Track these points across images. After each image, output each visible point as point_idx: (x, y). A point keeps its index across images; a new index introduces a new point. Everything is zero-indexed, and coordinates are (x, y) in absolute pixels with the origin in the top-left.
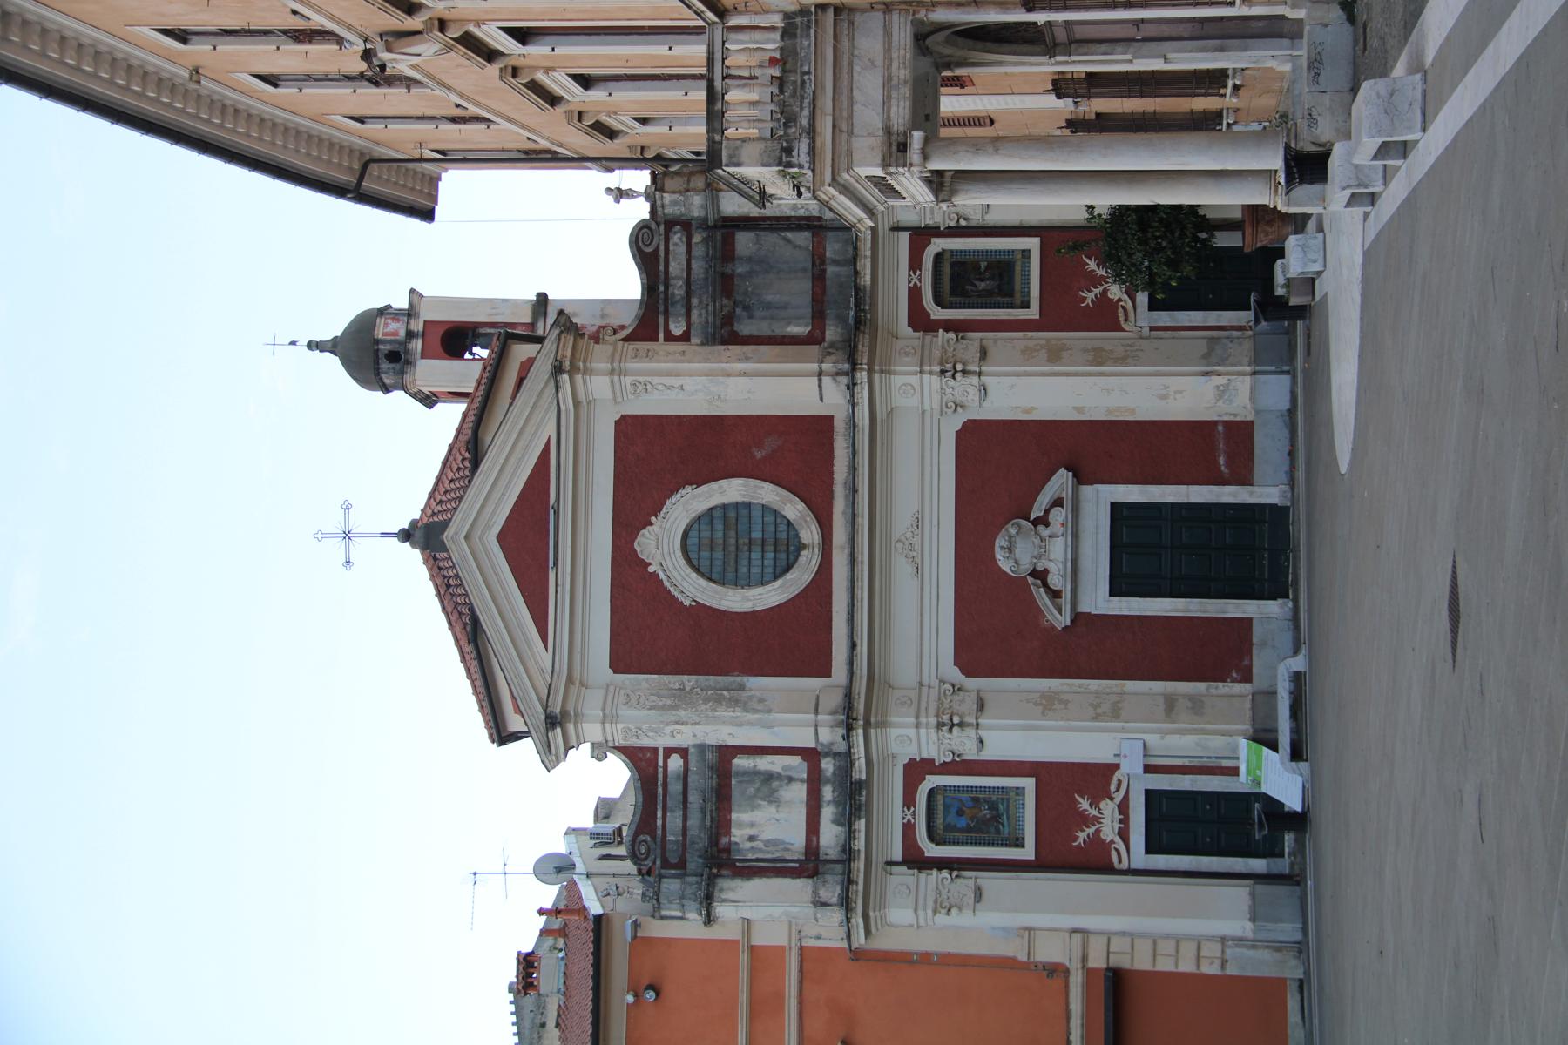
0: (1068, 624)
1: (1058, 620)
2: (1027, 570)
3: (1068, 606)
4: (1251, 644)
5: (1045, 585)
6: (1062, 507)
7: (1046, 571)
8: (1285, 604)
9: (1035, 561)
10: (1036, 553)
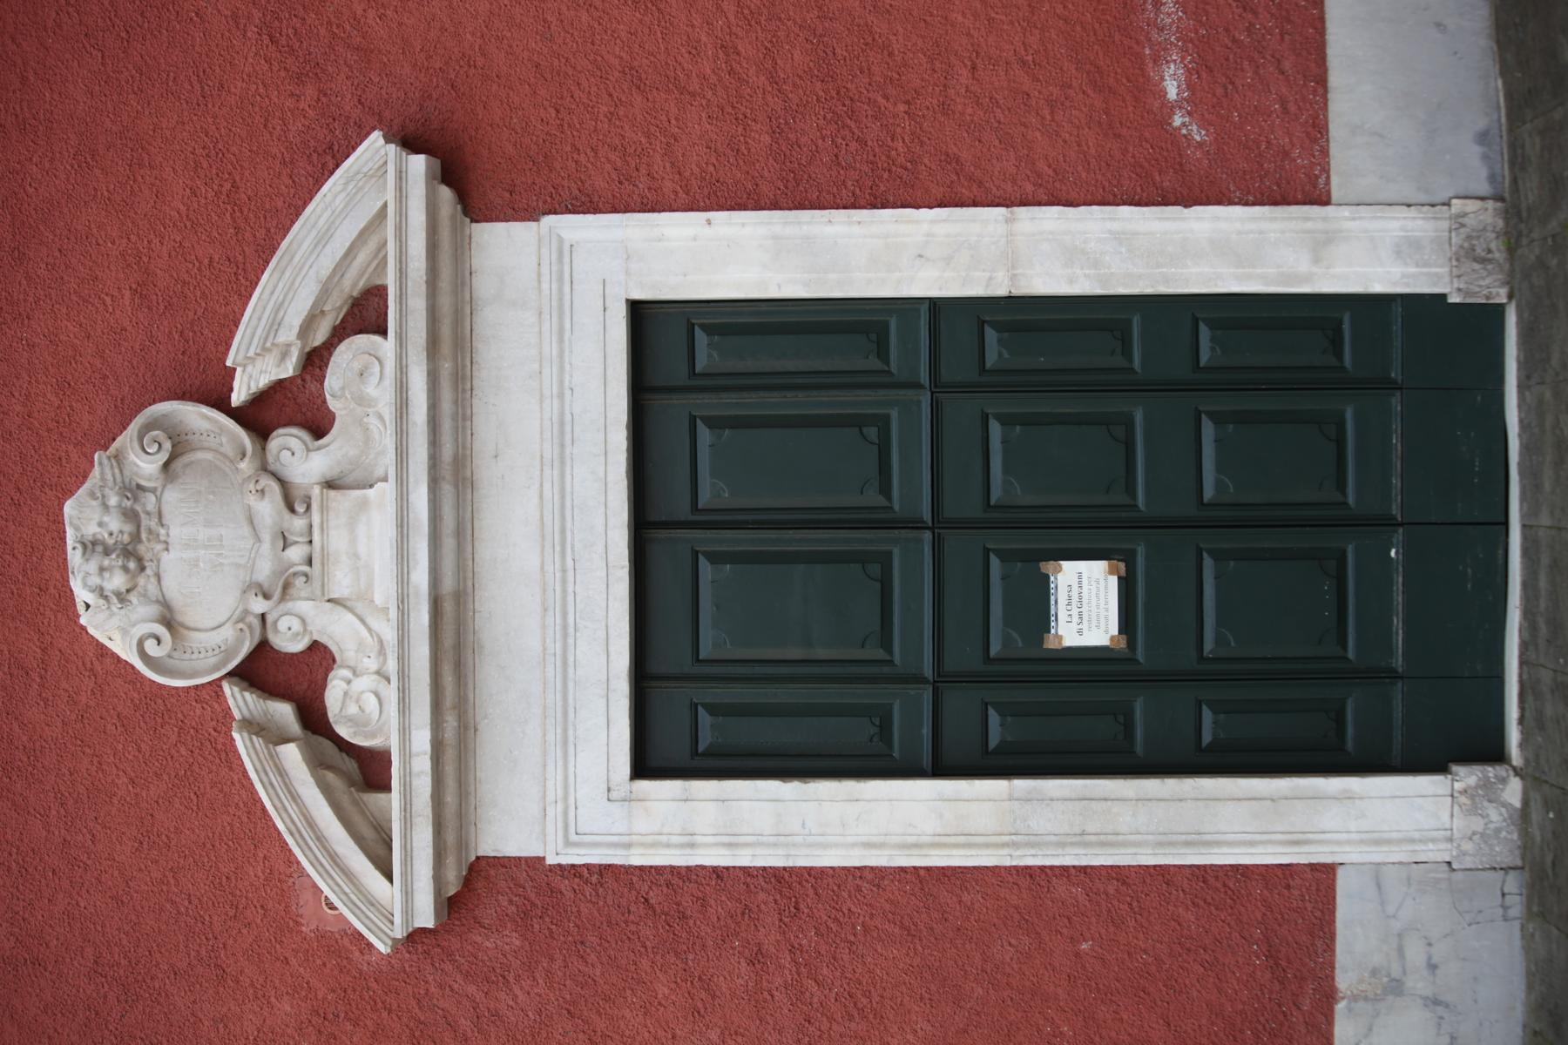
0: (425, 917)
1: (372, 903)
2: (228, 654)
3: (423, 837)
4: (1328, 996)
5: (314, 720)
6: (383, 332)
7: (319, 657)
8: (1488, 791)
9: (259, 605)
10: (264, 570)
